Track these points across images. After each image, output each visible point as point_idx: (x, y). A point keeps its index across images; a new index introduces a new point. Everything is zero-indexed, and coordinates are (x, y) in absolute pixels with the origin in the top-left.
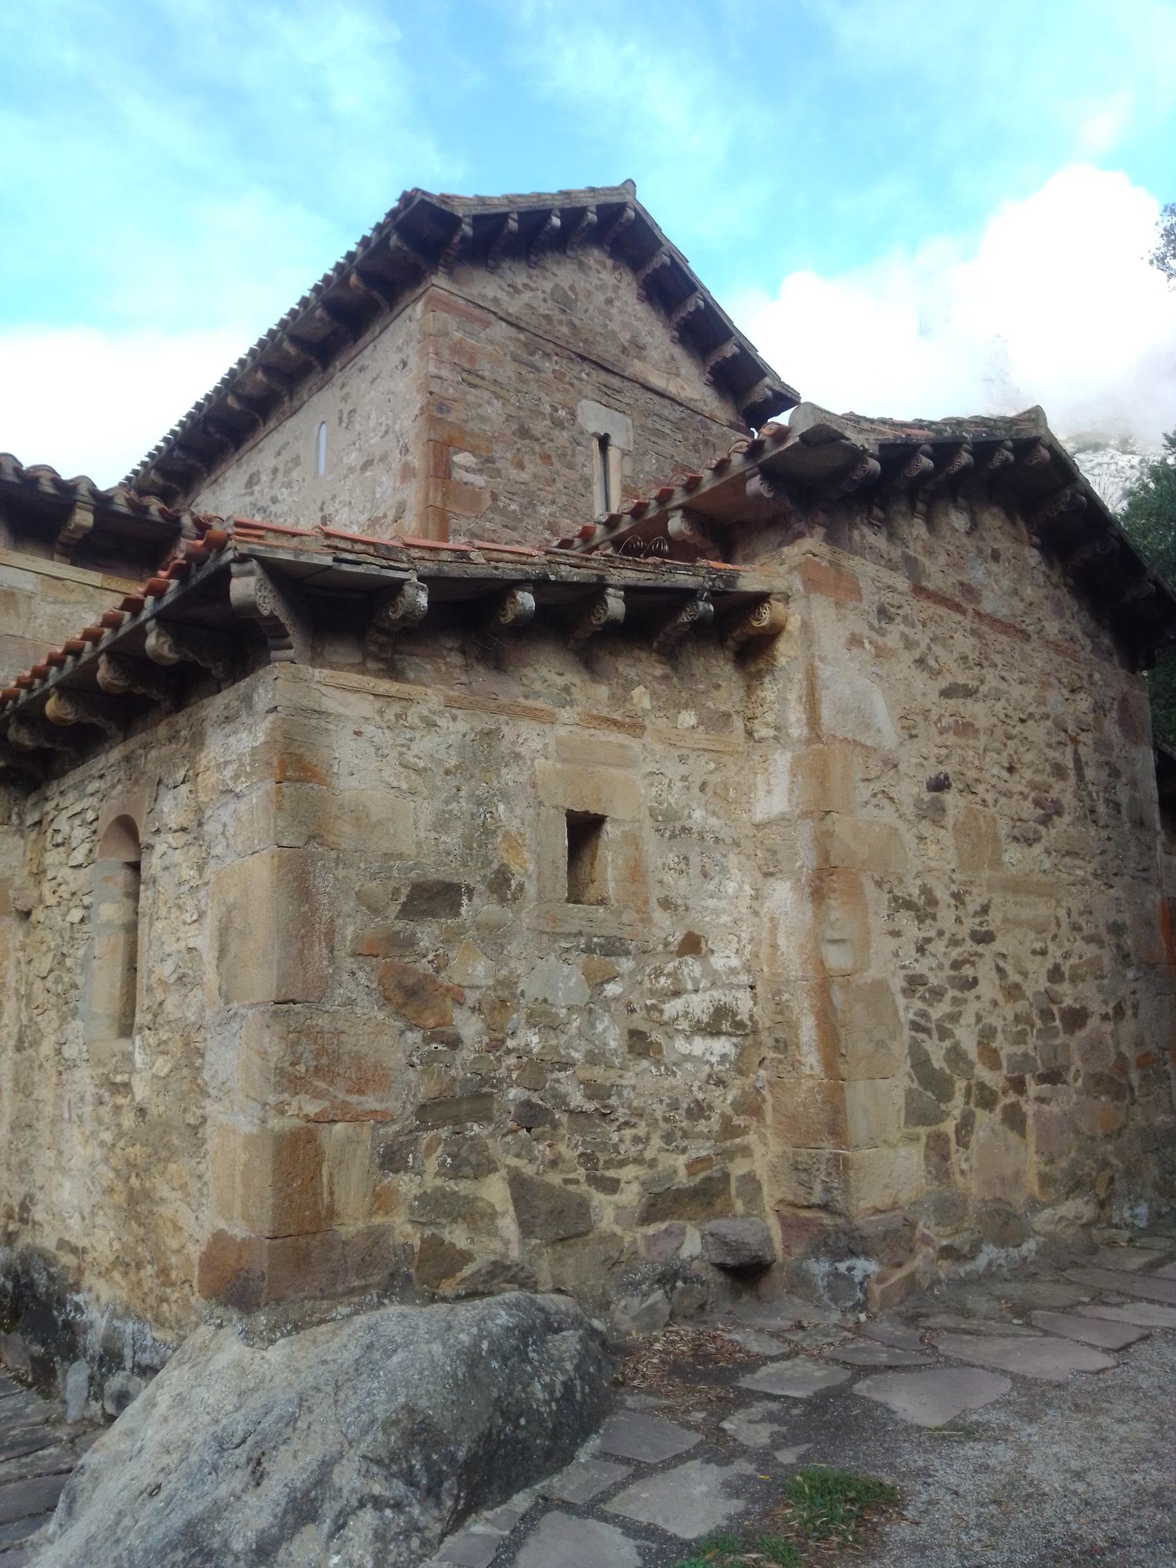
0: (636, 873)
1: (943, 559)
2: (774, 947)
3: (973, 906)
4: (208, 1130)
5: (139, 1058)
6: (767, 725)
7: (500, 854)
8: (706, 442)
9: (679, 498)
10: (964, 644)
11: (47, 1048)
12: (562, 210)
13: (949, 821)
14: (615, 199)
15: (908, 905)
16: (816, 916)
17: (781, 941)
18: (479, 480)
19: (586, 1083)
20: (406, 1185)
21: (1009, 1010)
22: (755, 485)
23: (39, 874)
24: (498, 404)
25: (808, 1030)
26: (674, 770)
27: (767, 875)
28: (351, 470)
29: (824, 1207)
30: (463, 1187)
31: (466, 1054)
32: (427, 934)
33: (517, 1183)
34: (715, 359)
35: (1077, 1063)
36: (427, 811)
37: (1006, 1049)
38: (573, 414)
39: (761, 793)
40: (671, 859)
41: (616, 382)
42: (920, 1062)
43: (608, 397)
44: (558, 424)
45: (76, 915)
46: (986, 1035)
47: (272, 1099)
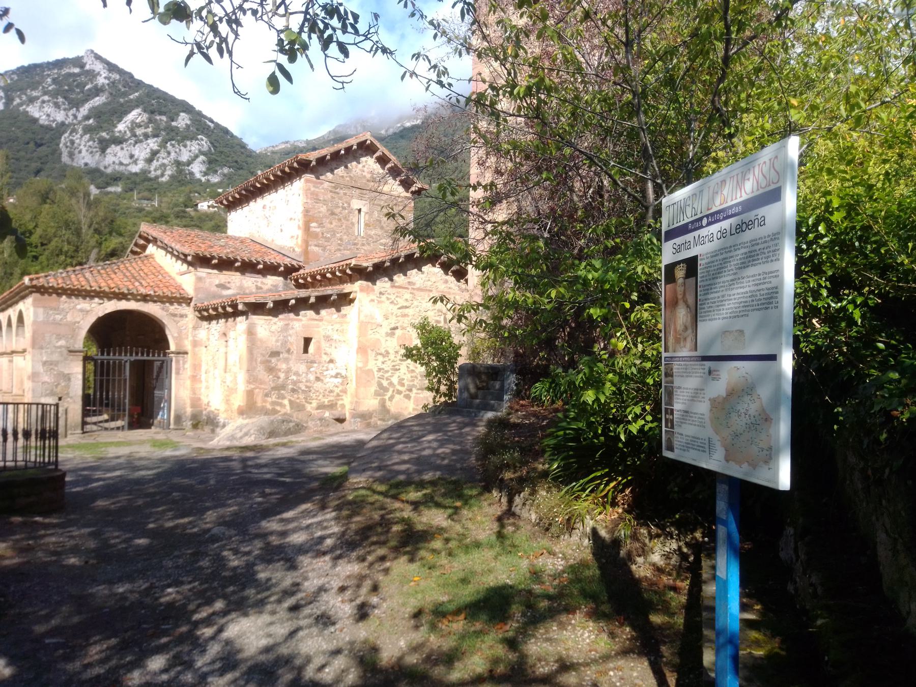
0: (319, 348)
7: (289, 346)
10: (407, 296)
13: (396, 336)
15: (381, 354)
18: (318, 230)
20: (269, 399)
21: (409, 376)
23: (208, 339)
26: (330, 327)
32: (274, 360)
33: (290, 400)
36: (274, 339)
37: (405, 382)
38: (349, 204)
41: (364, 192)
42: (380, 385)
43: (361, 198)
44: (344, 208)
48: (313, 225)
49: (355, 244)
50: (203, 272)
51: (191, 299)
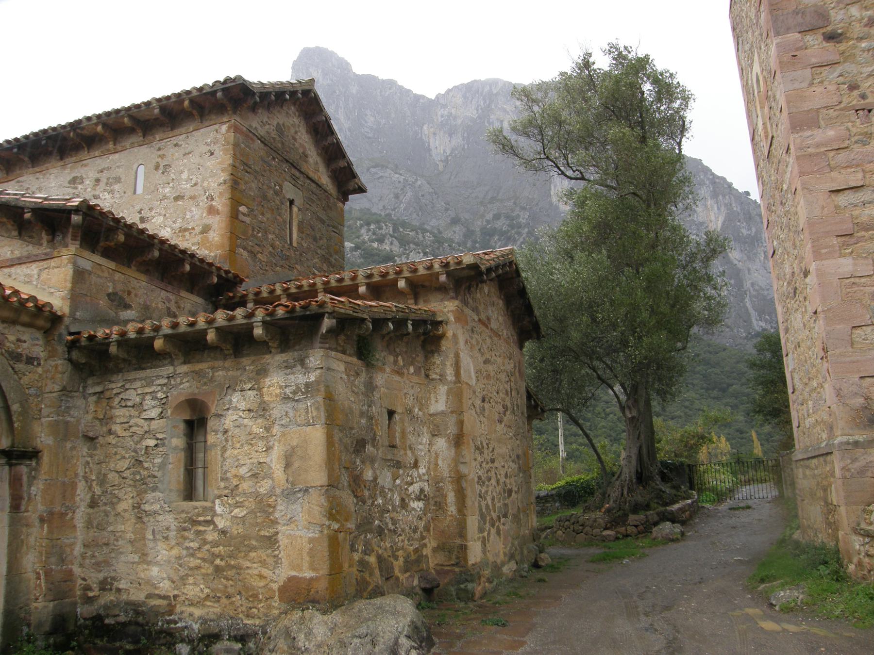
1: (483, 305)
2: (437, 465)
3: (491, 449)
4: (280, 536)
5: (219, 509)
6: (436, 373)
8: (328, 206)
9: (406, 274)
11: (124, 505)
12: (290, 91)
14: (307, 88)
16: (456, 453)
17: (440, 462)
18: (247, 220)
19: (392, 519)
22: (443, 278)
24: (256, 182)
25: (451, 497)
27: (434, 435)
28: (165, 197)
29: (457, 564)
30: (366, 557)
31: (366, 507)
34: (334, 166)
35: (510, 511)
39: (433, 402)
40: (411, 429)
41: (297, 174)
45: (152, 443)
46: (493, 499)
47: (327, 523)
48: (243, 209)
49: (287, 258)
50: (91, 260)
51: (56, 319)
